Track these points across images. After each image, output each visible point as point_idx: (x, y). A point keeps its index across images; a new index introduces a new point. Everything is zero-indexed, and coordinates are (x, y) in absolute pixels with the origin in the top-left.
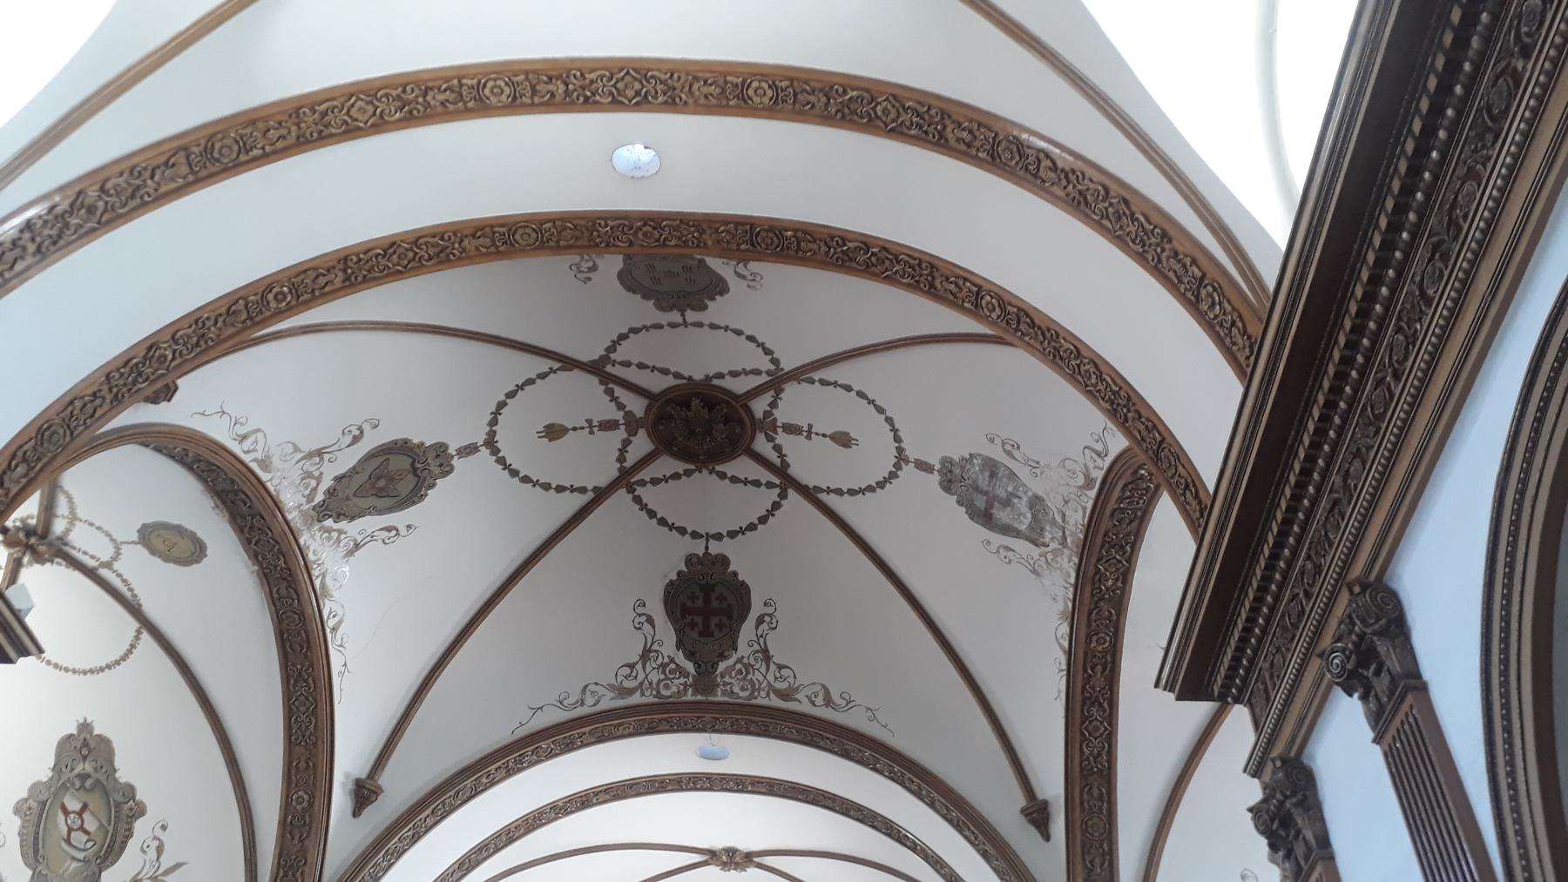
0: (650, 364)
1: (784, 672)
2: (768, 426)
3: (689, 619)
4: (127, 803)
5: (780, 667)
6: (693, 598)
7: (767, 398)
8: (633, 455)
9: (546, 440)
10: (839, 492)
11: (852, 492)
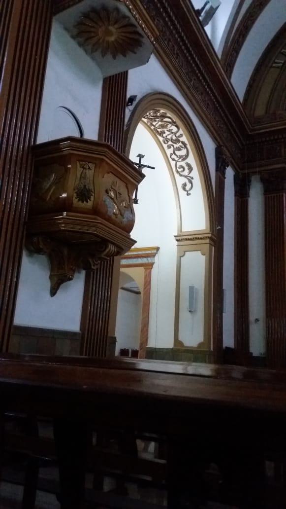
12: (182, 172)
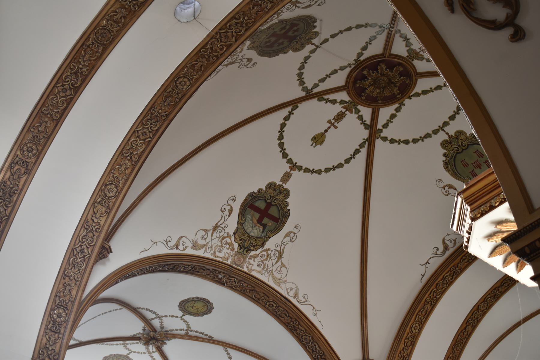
0: (435, 91)
2: (350, 107)
7: (367, 118)
10: (287, 118)
11: (283, 126)
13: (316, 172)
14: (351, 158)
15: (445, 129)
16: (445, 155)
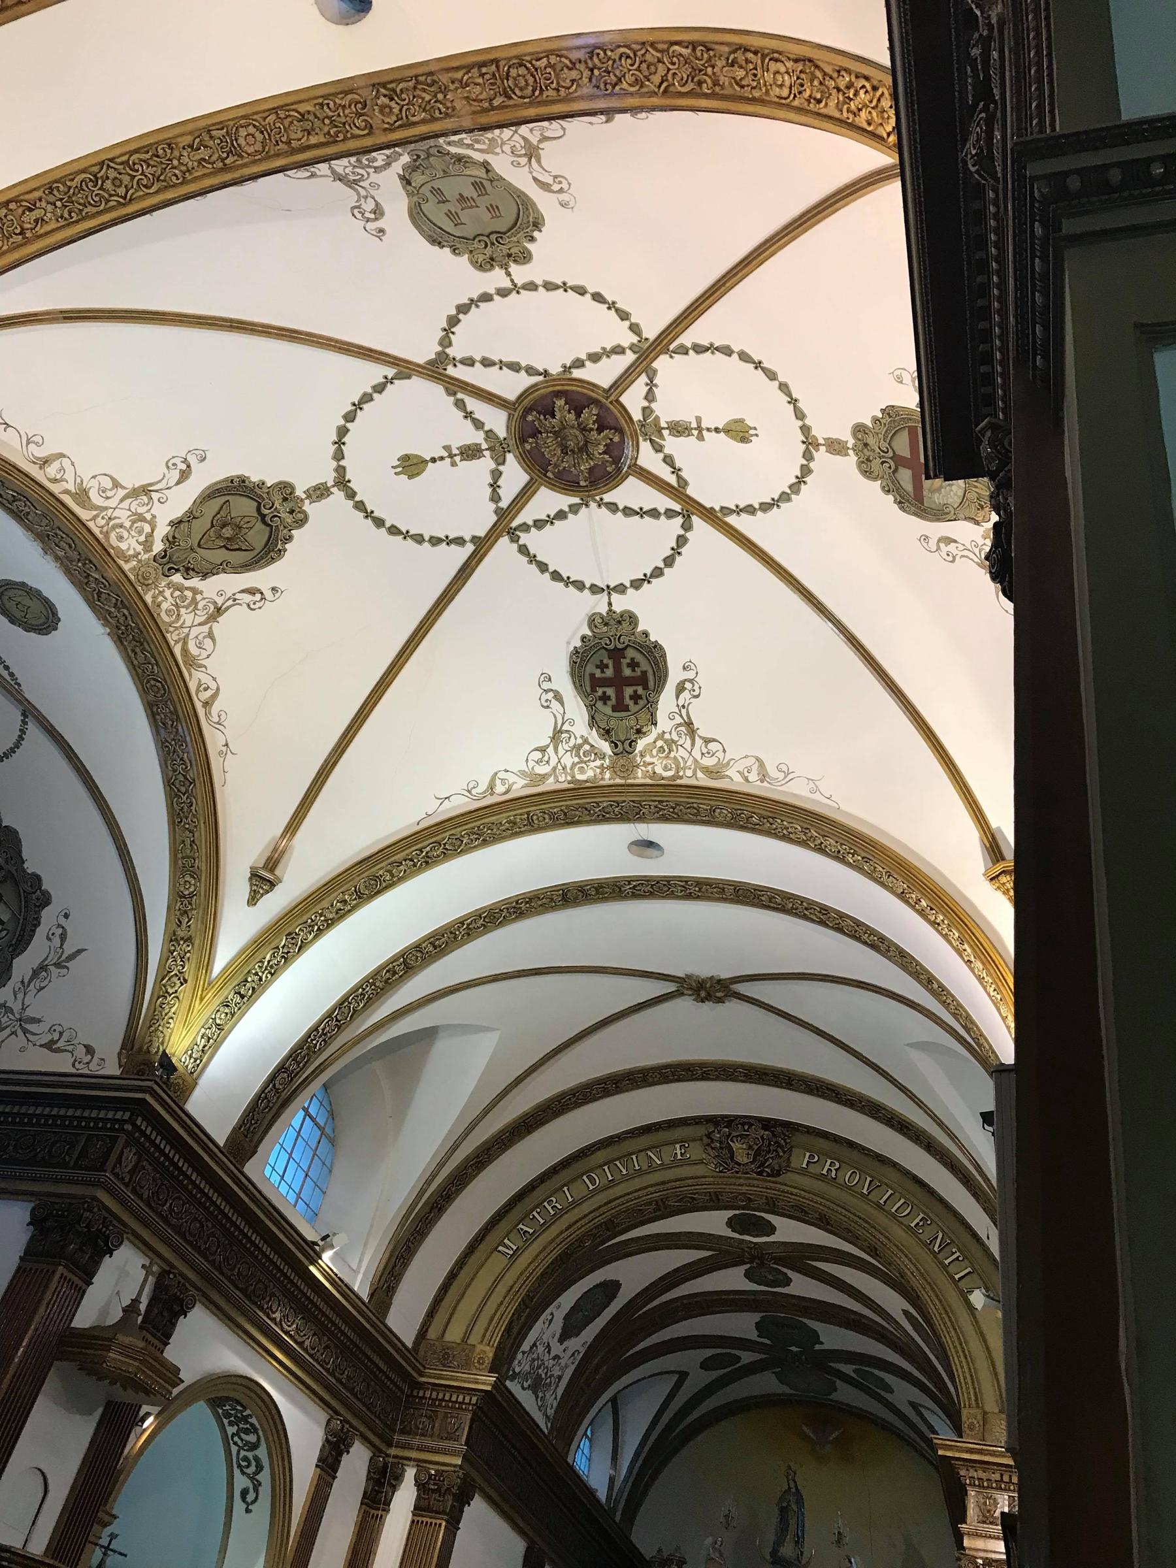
1: (713, 746)
2: (651, 429)
3: (600, 691)
4: (34, 893)
5: (707, 741)
6: (602, 667)
7: (639, 386)
8: (508, 495)
9: (404, 477)
10: (750, 510)
11: (766, 507)
12: (248, 1467)
13: (789, 395)
14: (717, 349)
15: (509, 285)
16: (532, 239)
